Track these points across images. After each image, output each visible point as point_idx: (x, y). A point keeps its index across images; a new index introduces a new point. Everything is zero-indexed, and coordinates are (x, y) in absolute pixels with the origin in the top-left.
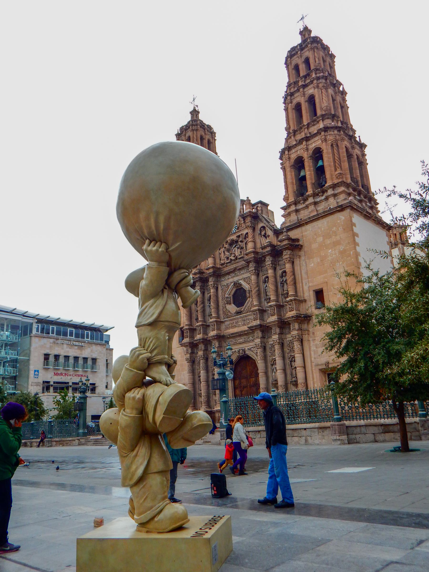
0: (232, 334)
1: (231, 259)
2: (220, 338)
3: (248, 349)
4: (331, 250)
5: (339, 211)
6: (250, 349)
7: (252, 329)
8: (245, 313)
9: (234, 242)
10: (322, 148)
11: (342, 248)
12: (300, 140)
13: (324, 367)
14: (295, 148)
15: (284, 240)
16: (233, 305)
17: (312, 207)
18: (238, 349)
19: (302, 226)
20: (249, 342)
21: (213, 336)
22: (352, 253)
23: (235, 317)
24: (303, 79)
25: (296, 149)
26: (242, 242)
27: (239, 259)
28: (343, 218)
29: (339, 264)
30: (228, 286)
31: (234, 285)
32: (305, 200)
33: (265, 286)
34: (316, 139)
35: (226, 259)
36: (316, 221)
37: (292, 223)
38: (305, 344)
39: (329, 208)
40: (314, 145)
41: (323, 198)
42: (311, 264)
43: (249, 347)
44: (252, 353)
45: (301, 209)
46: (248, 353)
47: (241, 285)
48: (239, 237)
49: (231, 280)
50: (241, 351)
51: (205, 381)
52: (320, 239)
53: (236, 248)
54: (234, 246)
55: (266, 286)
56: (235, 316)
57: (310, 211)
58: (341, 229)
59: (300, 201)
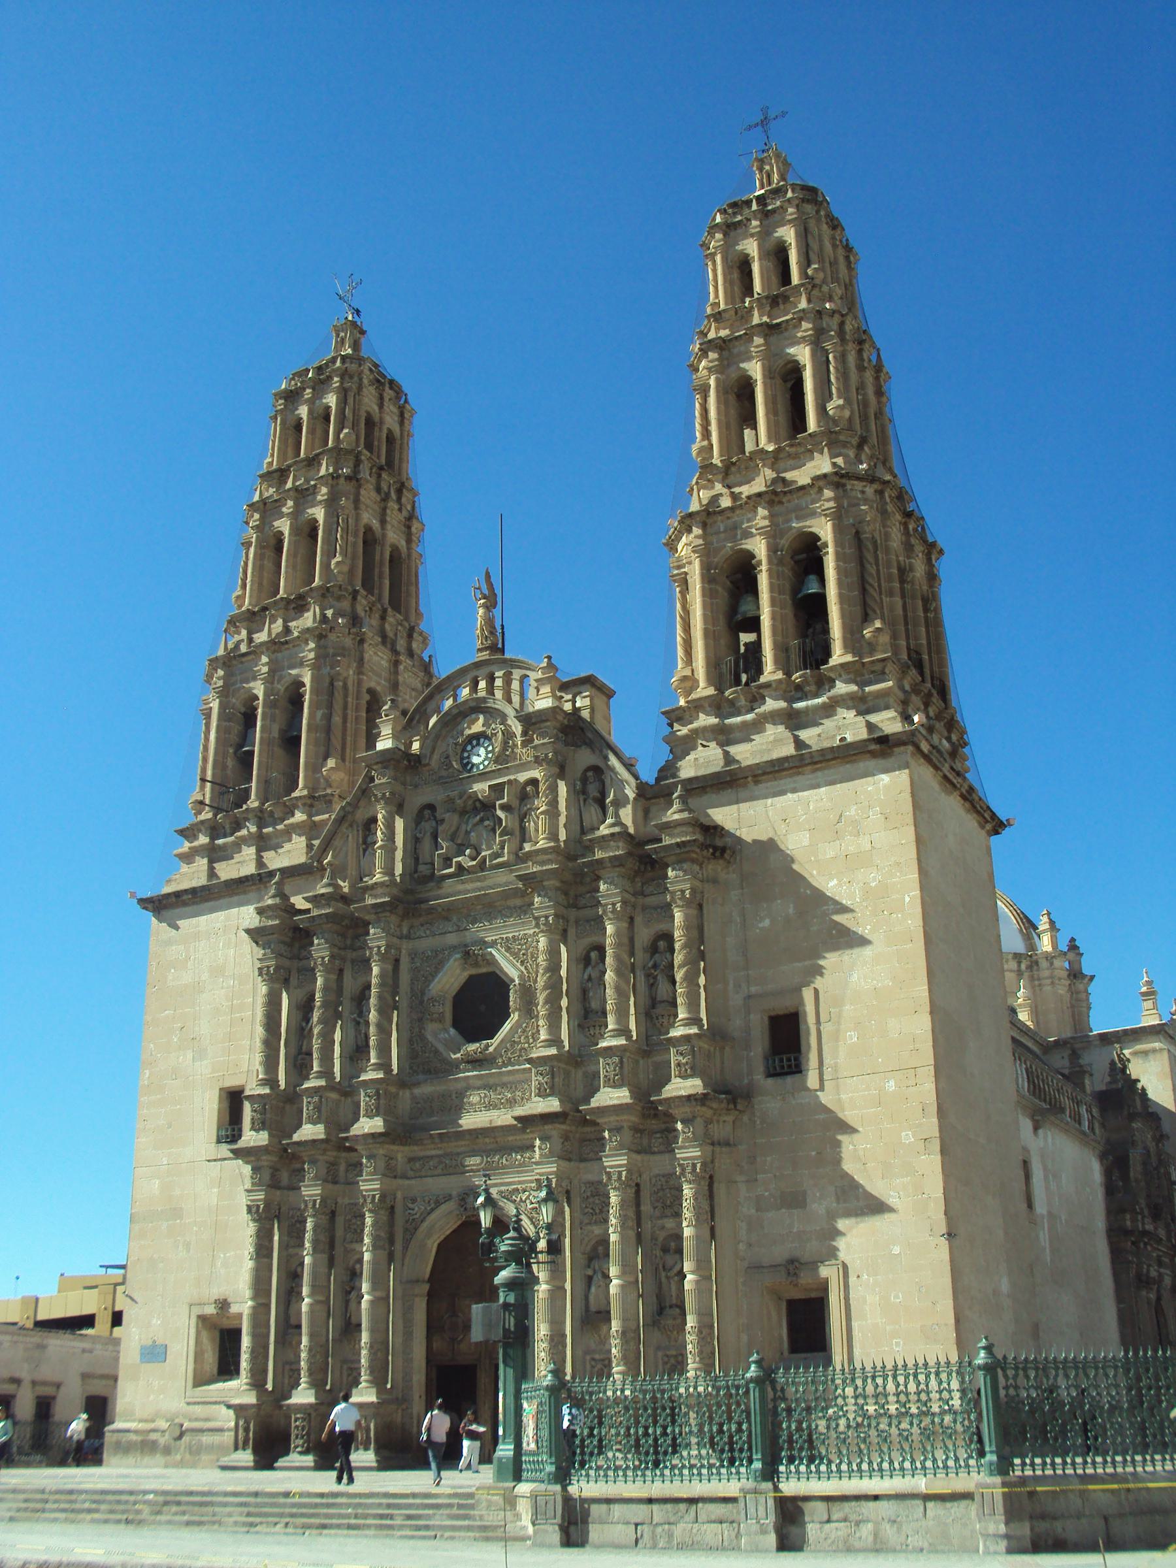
4: (835, 882)
9: (478, 804)
10: (823, 540)
11: (874, 879)
12: (749, 497)
15: (675, 827)
16: (452, 1031)
22: (907, 899)
24: (768, 308)
30: (436, 961)
32: (756, 699)
33: (586, 977)
37: (701, 773)
38: (720, 1190)
39: (839, 738)
42: (762, 919)
43: (503, 1188)
48: (497, 789)
54: (478, 817)
55: (590, 976)
57: (771, 738)
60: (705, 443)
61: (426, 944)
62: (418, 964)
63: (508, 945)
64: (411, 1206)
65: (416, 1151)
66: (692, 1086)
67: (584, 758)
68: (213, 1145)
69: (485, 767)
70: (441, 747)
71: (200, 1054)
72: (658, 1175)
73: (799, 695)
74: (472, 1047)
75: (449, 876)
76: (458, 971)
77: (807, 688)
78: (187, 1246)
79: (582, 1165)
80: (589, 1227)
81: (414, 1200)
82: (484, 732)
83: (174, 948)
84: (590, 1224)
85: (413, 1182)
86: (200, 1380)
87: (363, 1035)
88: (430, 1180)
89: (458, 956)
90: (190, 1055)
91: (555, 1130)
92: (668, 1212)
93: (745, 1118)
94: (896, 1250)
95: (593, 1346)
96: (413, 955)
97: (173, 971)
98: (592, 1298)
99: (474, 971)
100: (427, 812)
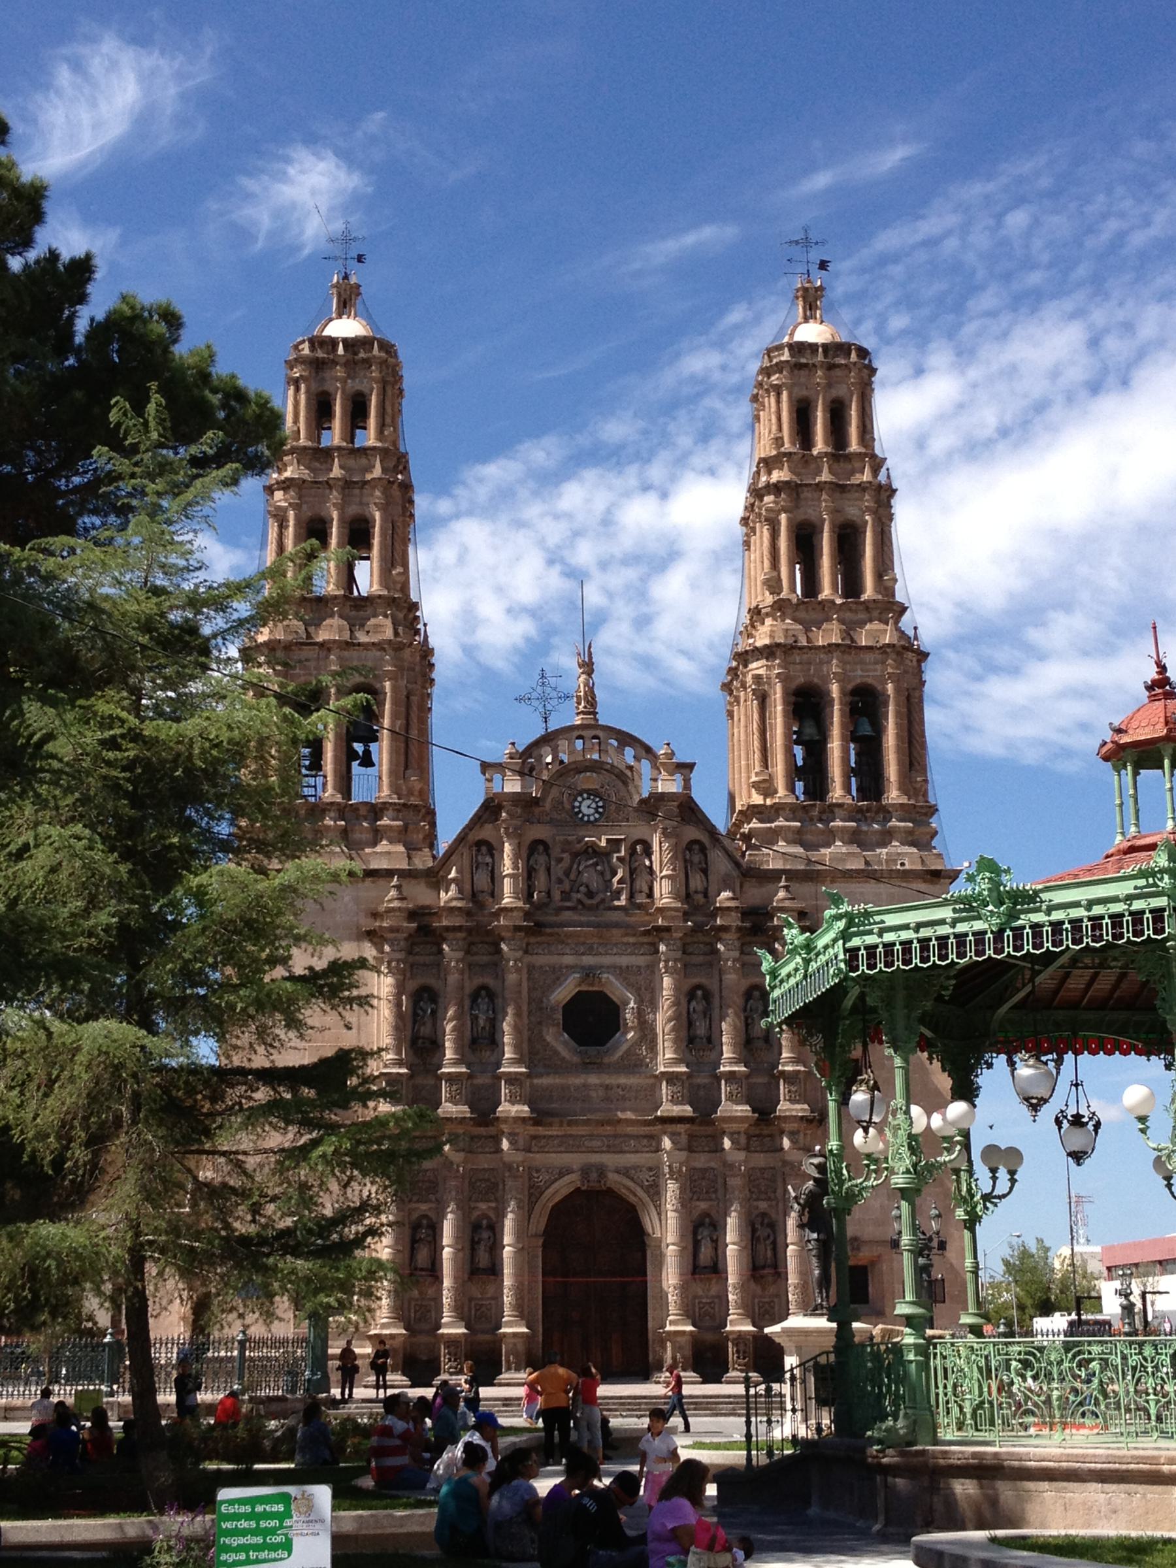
1: (580, 901)
6: (625, 1172)
30: (557, 975)
35: (557, 895)
44: (630, 1184)
53: (591, 870)
60: (775, 574)
61: (541, 960)
63: (623, 973)
65: (541, 1130)
66: (801, 1109)
67: (692, 833)
69: (596, 820)
70: (554, 792)
72: (753, 1168)
75: (568, 908)
76: (572, 986)
79: (694, 1155)
80: (698, 1203)
81: (538, 1171)
84: (698, 1200)
85: (538, 1156)
88: (553, 1155)
89: (577, 975)
91: (681, 1128)
92: (763, 1196)
93: (819, 1132)
95: (701, 1293)
96: (531, 968)
98: (702, 1256)
99: (584, 988)
100: (541, 848)
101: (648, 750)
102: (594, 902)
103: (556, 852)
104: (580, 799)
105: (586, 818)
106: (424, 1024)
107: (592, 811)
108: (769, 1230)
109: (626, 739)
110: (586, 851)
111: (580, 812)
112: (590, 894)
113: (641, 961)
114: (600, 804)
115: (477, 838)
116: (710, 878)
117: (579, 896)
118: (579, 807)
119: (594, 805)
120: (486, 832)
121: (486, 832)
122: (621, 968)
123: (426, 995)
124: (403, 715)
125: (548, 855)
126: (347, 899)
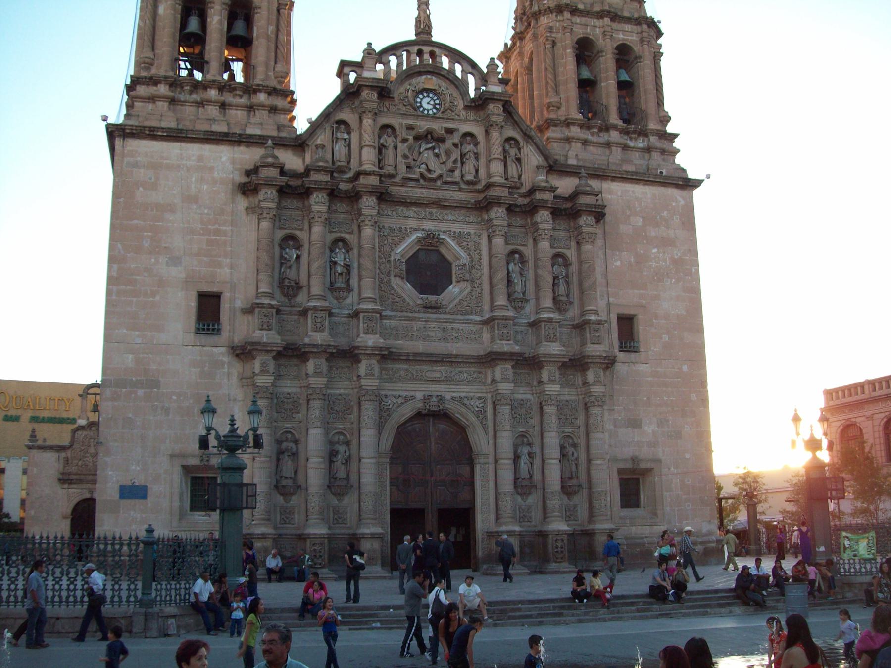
0: (415, 354)
1: (422, 175)
2: (386, 356)
3: (453, 398)
5: (677, 186)
7: (491, 359)
8: (449, 313)
9: (429, 136)
13: (629, 465)
14: (582, 16)
15: (588, 195)
17: (617, 154)
18: (427, 394)
19: (602, 179)
20: (458, 382)
21: (381, 349)
23: (417, 315)
25: (584, 20)
26: (455, 145)
27: (446, 183)
28: (682, 203)
29: (671, 283)
30: (403, 234)
31: (425, 238)
34: (628, 27)
35: (402, 168)
36: (631, 183)
40: (621, 36)
41: (641, 144)
42: (615, 261)
43: (455, 395)
44: (463, 410)
45: (593, 143)
46: (450, 406)
47: (442, 242)
48: (450, 131)
49: (412, 223)
50: (434, 399)
51: (321, 457)
52: (639, 221)
53: (430, 152)
54: (430, 146)
56: (419, 312)
58: (677, 218)
59: (594, 127)
62: (386, 234)
64: (384, 399)
68: (192, 334)
69: (434, 113)
71: (175, 261)
73: (626, 137)
74: (432, 298)
77: (633, 136)
78: (167, 411)
81: (386, 396)
82: (434, 90)
83: (142, 170)
86: (182, 516)
87: (337, 274)
90: (163, 259)
94: (687, 456)
97: (141, 189)
100: (389, 130)
101: (474, 65)
102: (434, 176)
103: (402, 133)
104: (421, 96)
105: (426, 112)
106: (290, 267)
107: (431, 107)
108: (573, 449)
109: (457, 56)
110: (426, 136)
111: (421, 106)
112: (429, 171)
113: (471, 229)
114: (437, 102)
115: (337, 118)
116: (523, 168)
117: (422, 170)
118: (420, 103)
119: (432, 103)
120: (345, 115)
121: (345, 115)
122: (455, 232)
123: (291, 243)
124: (274, 23)
125: (396, 137)
126: (224, 159)
